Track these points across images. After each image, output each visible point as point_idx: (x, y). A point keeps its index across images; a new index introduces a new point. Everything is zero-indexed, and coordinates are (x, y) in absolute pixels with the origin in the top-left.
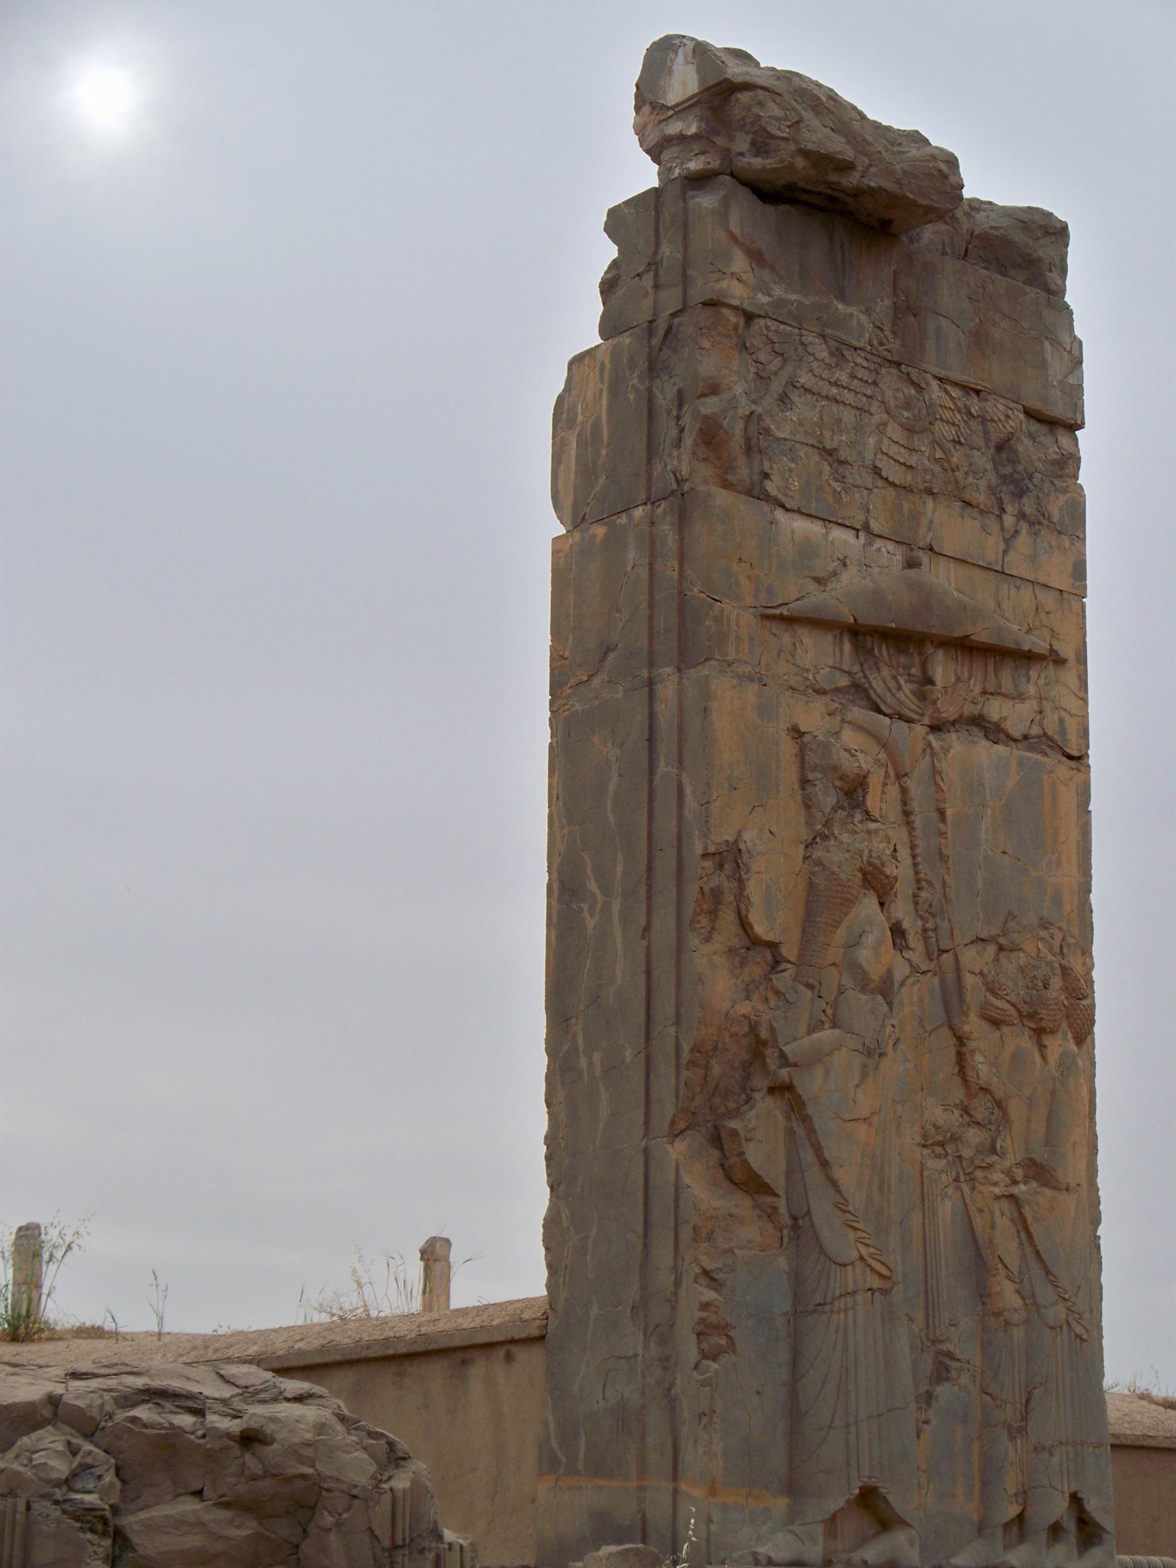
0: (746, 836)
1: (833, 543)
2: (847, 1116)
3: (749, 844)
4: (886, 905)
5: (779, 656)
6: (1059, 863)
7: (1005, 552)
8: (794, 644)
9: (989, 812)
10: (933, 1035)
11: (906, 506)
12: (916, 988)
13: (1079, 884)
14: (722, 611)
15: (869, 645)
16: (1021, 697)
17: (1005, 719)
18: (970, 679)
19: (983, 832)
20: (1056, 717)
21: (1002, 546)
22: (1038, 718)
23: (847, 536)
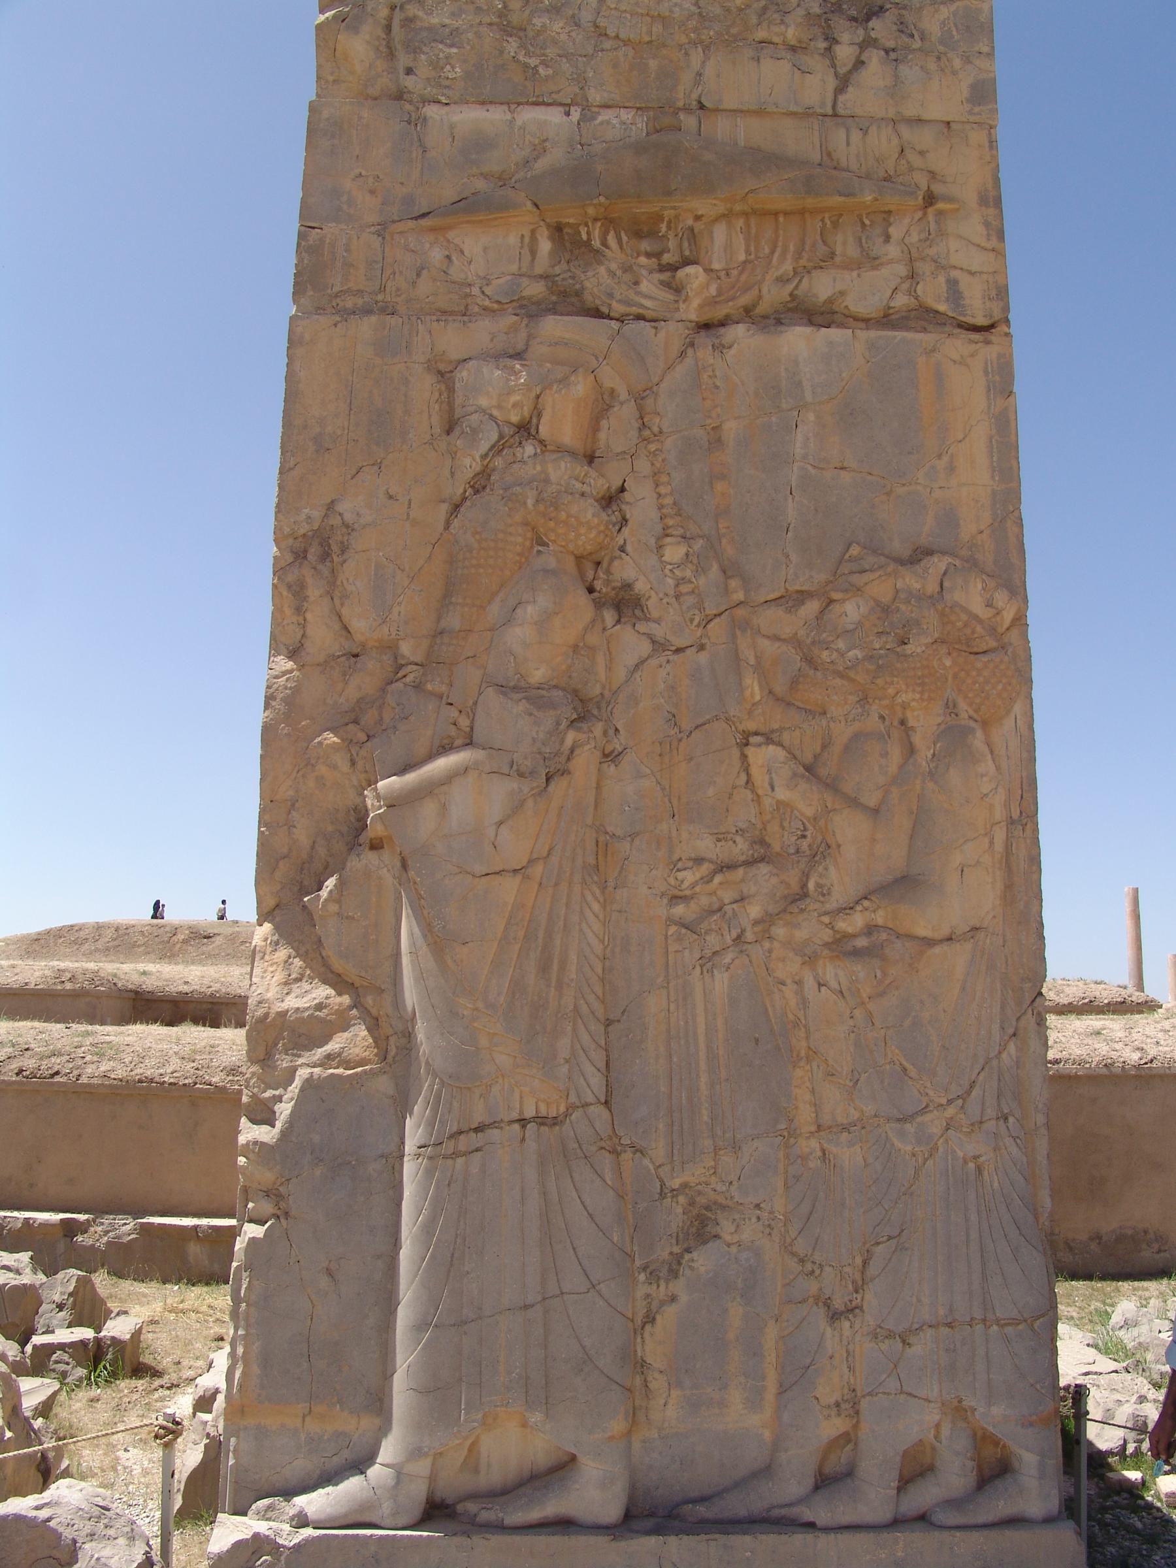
0: (346, 507)
1: (523, 128)
2: (480, 869)
3: (348, 517)
4: (605, 565)
5: (418, 275)
6: (951, 469)
7: (840, 90)
8: (448, 257)
9: (811, 417)
10: (696, 735)
11: (653, 64)
12: (662, 673)
13: (994, 493)
14: (322, 240)
15: (584, 237)
16: (873, 261)
17: (842, 293)
18: (773, 252)
19: (798, 445)
20: (942, 279)
21: (832, 83)
22: (905, 286)
23: (554, 116)
